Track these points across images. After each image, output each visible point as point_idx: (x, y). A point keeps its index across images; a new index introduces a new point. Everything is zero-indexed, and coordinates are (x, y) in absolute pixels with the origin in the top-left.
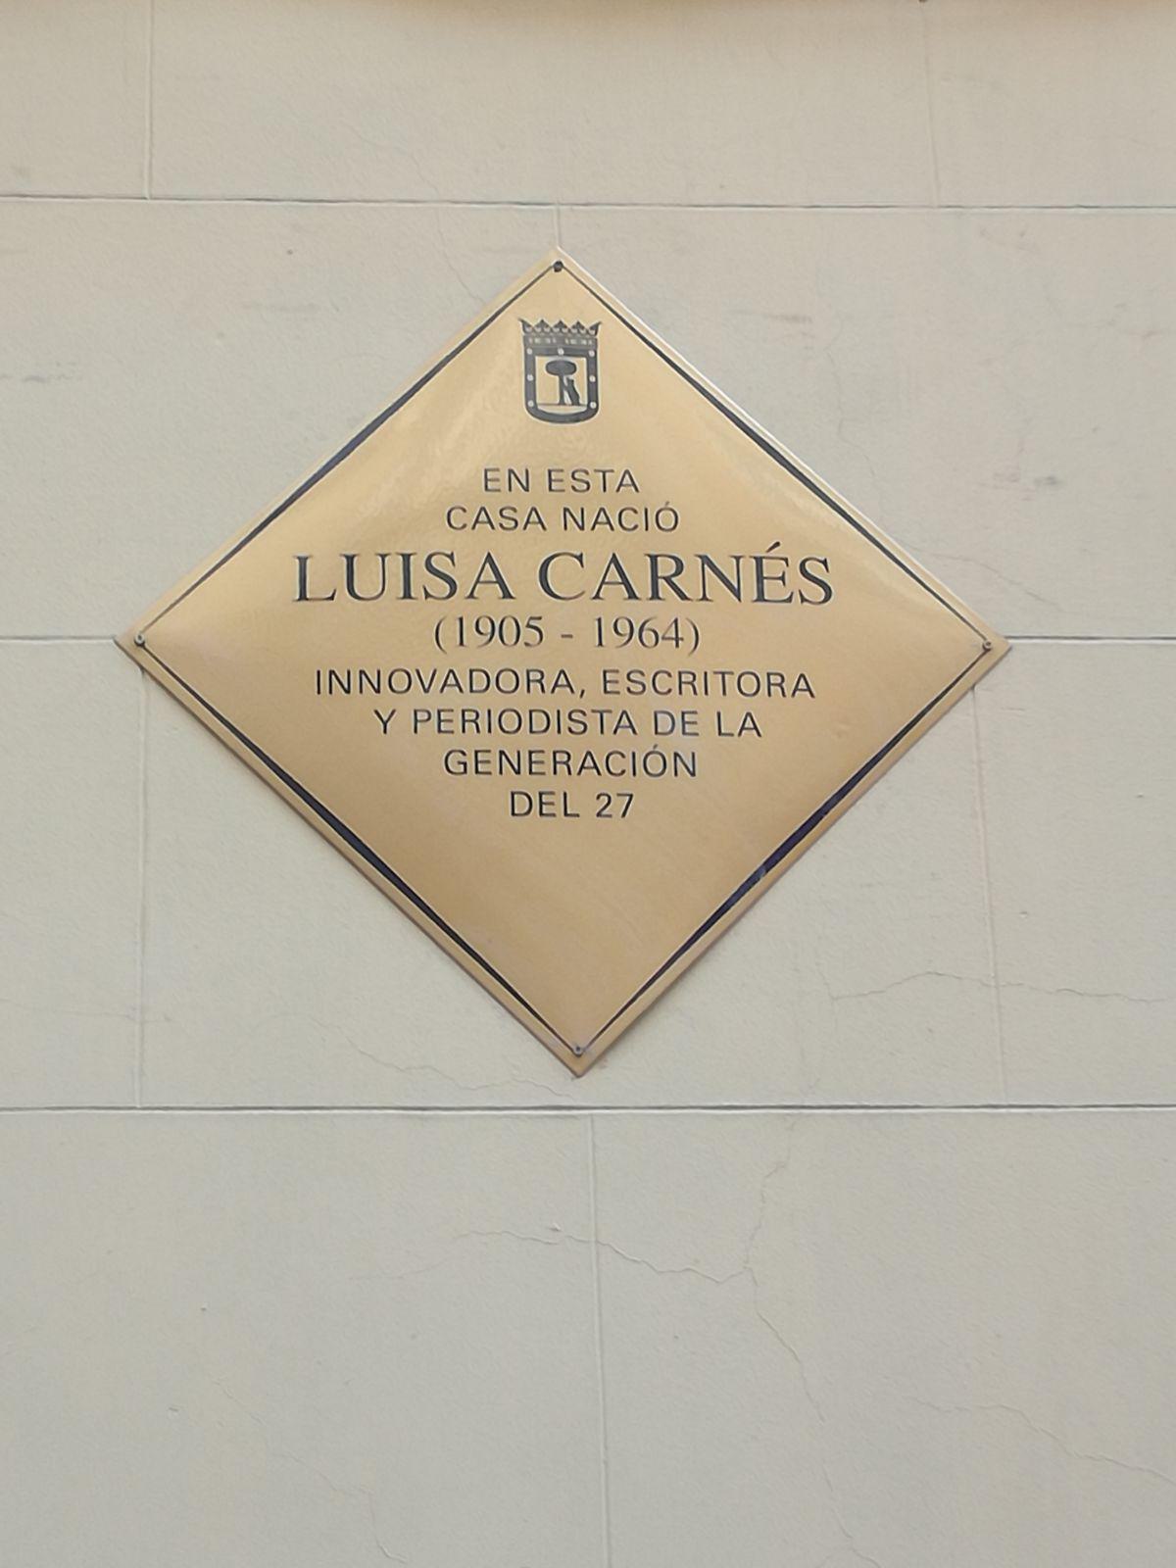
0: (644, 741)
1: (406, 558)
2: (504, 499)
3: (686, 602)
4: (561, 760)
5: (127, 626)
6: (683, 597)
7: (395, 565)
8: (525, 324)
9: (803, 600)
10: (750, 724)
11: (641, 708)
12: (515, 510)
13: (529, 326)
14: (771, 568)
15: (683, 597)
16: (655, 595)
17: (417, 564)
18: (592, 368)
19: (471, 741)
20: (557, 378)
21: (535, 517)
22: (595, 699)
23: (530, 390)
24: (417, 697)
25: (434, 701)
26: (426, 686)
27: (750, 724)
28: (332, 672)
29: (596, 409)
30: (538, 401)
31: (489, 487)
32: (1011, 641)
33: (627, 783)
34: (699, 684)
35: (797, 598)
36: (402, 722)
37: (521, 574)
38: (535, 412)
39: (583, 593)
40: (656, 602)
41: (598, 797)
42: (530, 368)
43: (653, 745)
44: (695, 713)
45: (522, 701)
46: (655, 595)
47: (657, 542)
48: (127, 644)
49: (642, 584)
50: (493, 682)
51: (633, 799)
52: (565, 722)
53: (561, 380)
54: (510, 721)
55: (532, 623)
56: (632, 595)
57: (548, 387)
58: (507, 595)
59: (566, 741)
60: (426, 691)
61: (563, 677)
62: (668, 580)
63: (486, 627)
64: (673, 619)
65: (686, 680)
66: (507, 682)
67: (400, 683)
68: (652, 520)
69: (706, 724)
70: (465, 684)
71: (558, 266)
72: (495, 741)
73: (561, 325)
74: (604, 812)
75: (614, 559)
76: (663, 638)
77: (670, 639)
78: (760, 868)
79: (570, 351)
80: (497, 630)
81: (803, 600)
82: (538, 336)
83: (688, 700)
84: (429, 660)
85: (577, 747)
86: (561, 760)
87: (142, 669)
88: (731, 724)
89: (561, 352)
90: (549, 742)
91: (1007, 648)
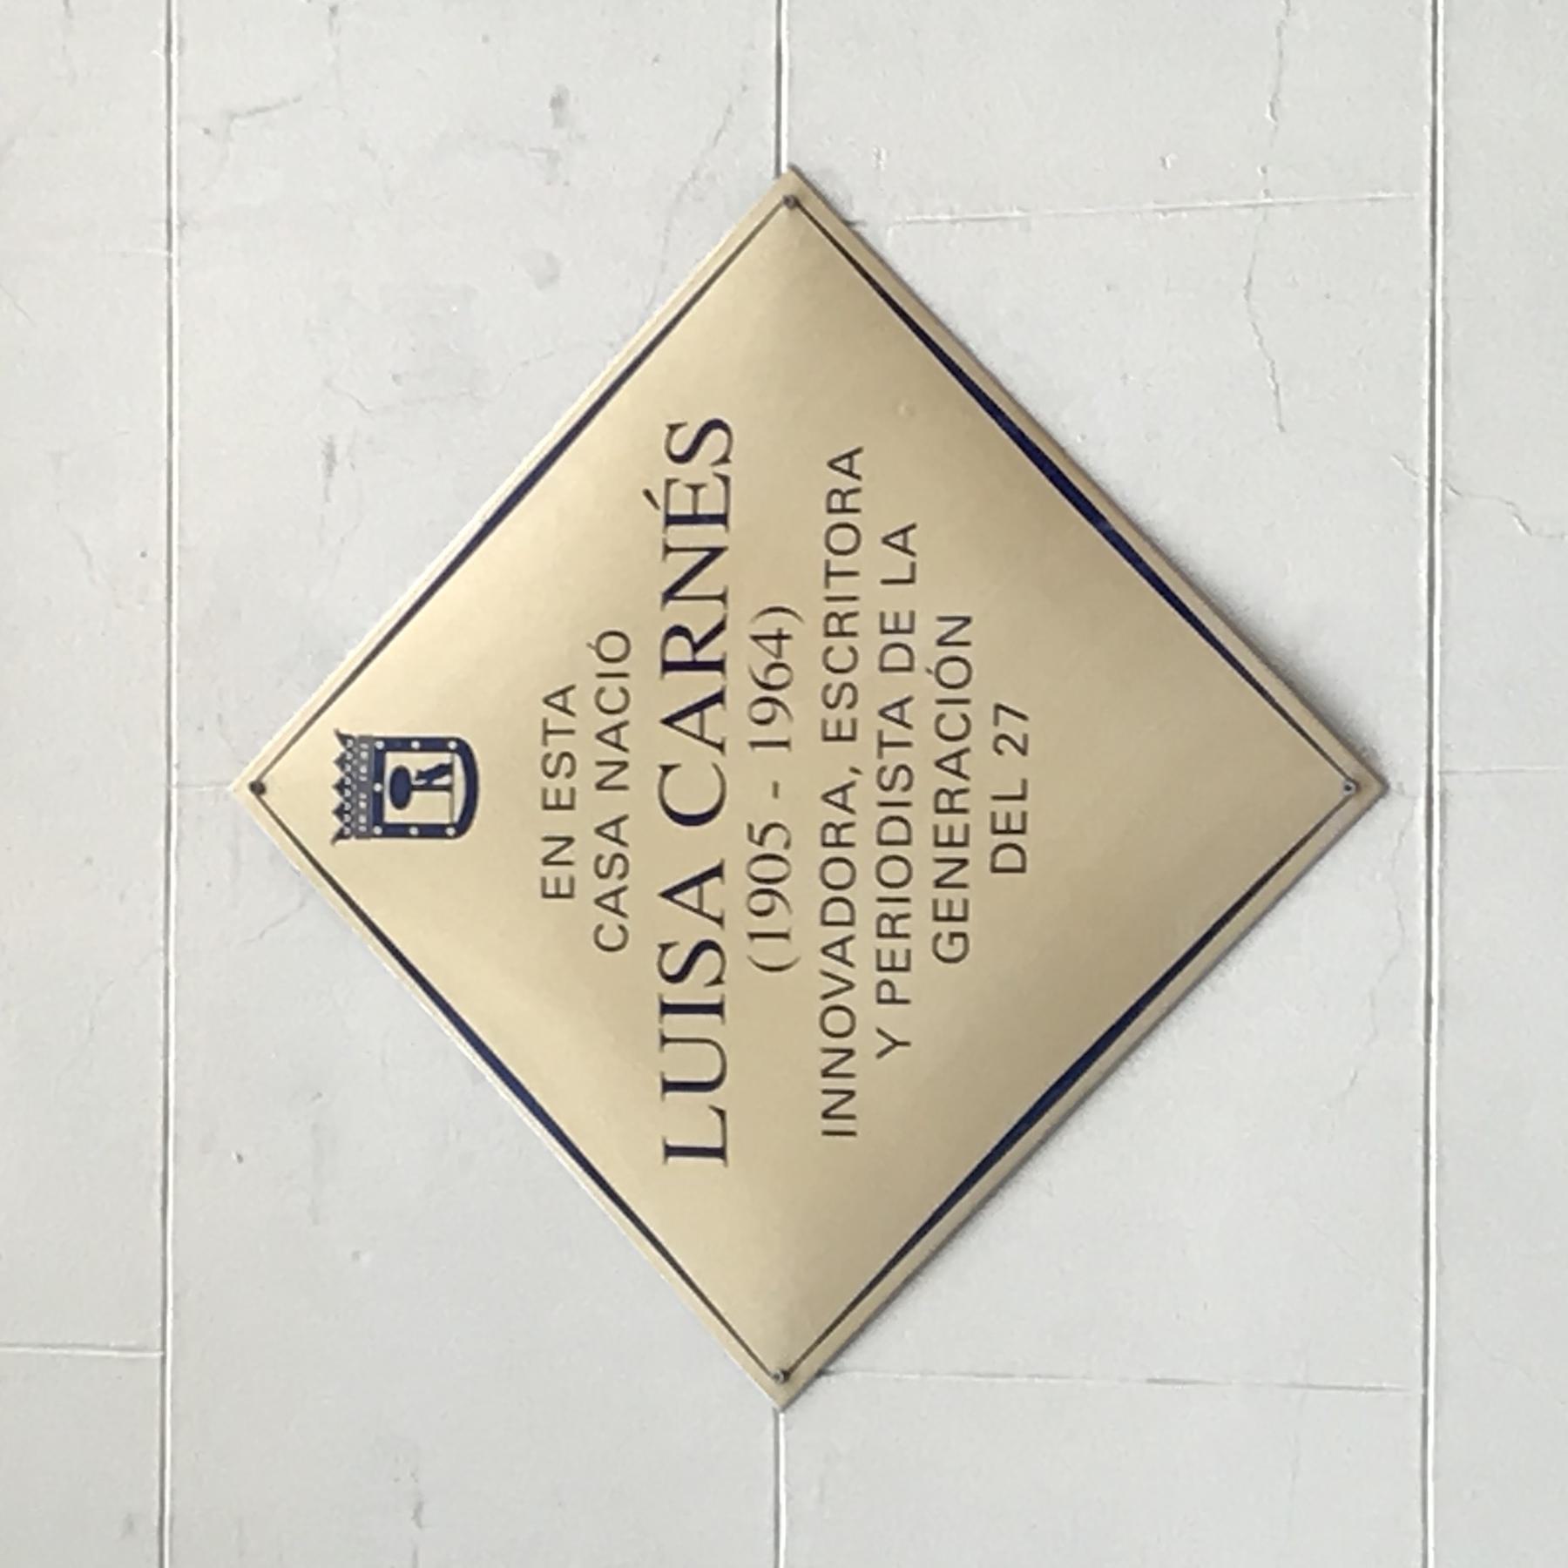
0: (921, 686)
1: (666, 1009)
2: (583, 872)
3: (729, 624)
4: (947, 803)
5: (762, 1396)
6: (720, 628)
7: (677, 1025)
8: (340, 835)
9: (725, 460)
10: (898, 539)
11: (876, 690)
12: (599, 858)
13: (342, 831)
14: (681, 507)
15: (720, 628)
16: (718, 666)
17: (677, 994)
18: (402, 745)
19: (920, 926)
20: (416, 795)
21: (611, 829)
22: (864, 751)
23: (432, 831)
24: (860, 999)
25: (865, 976)
26: (843, 985)
27: (898, 539)
28: (826, 1115)
29: (458, 741)
30: (446, 821)
31: (1019, 827)
32: (784, 169)
33: (980, 712)
34: (842, 608)
35: (723, 469)
36: (893, 1019)
37: (697, 850)
38: (462, 826)
39: (716, 767)
40: (728, 665)
41: (1000, 752)
42: (400, 831)
43: (927, 675)
44: (882, 616)
45: (865, 853)
46: (718, 666)
47: (644, 660)
48: (783, 1392)
49: (703, 684)
50: (838, 894)
51: (1004, 704)
52: (895, 795)
53: (421, 788)
54: (894, 872)
55: (757, 837)
56: (718, 698)
57: (426, 807)
58: (717, 872)
59: (922, 795)
60: (850, 986)
61: (837, 796)
62: (696, 648)
63: (763, 902)
64: (753, 644)
65: (837, 627)
66: (838, 874)
67: (837, 1021)
68: (613, 668)
69: (898, 600)
70: (840, 933)
71: (258, 788)
72: (921, 892)
73: (340, 787)
74: (1020, 742)
75: (669, 721)
76: (779, 655)
77: (780, 647)
78: (1100, 530)
79: (378, 776)
80: (767, 887)
81: (725, 460)
82: (355, 818)
83: (866, 624)
84: (809, 978)
85: (930, 780)
86: (947, 803)
87: (821, 1373)
88: (899, 565)
89: (378, 787)
90: (923, 818)
91: (793, 175)
